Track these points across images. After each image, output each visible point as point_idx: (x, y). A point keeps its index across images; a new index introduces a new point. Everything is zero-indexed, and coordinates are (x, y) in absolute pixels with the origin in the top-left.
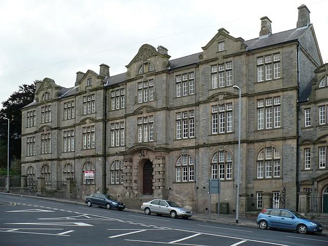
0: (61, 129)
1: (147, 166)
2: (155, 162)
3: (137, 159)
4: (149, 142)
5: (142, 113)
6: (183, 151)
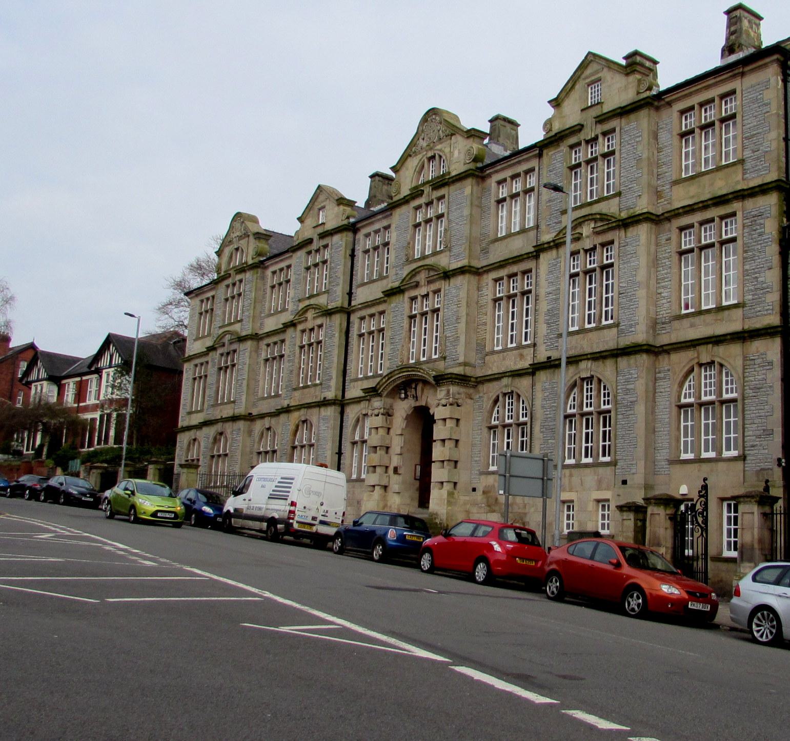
0: (262, 339)
1: (423, 420)
2: (438, 413)
3: (403, 408)
4: (418, 362)
5: (417, 285)
6: (505, 381)
